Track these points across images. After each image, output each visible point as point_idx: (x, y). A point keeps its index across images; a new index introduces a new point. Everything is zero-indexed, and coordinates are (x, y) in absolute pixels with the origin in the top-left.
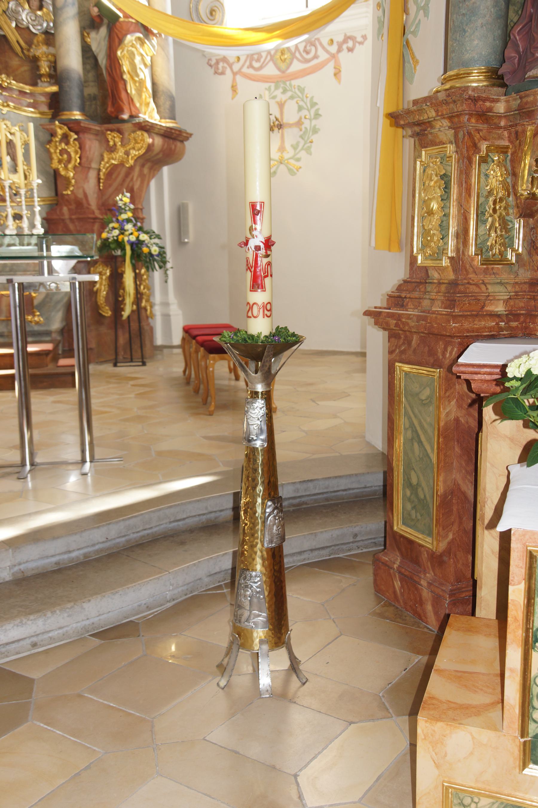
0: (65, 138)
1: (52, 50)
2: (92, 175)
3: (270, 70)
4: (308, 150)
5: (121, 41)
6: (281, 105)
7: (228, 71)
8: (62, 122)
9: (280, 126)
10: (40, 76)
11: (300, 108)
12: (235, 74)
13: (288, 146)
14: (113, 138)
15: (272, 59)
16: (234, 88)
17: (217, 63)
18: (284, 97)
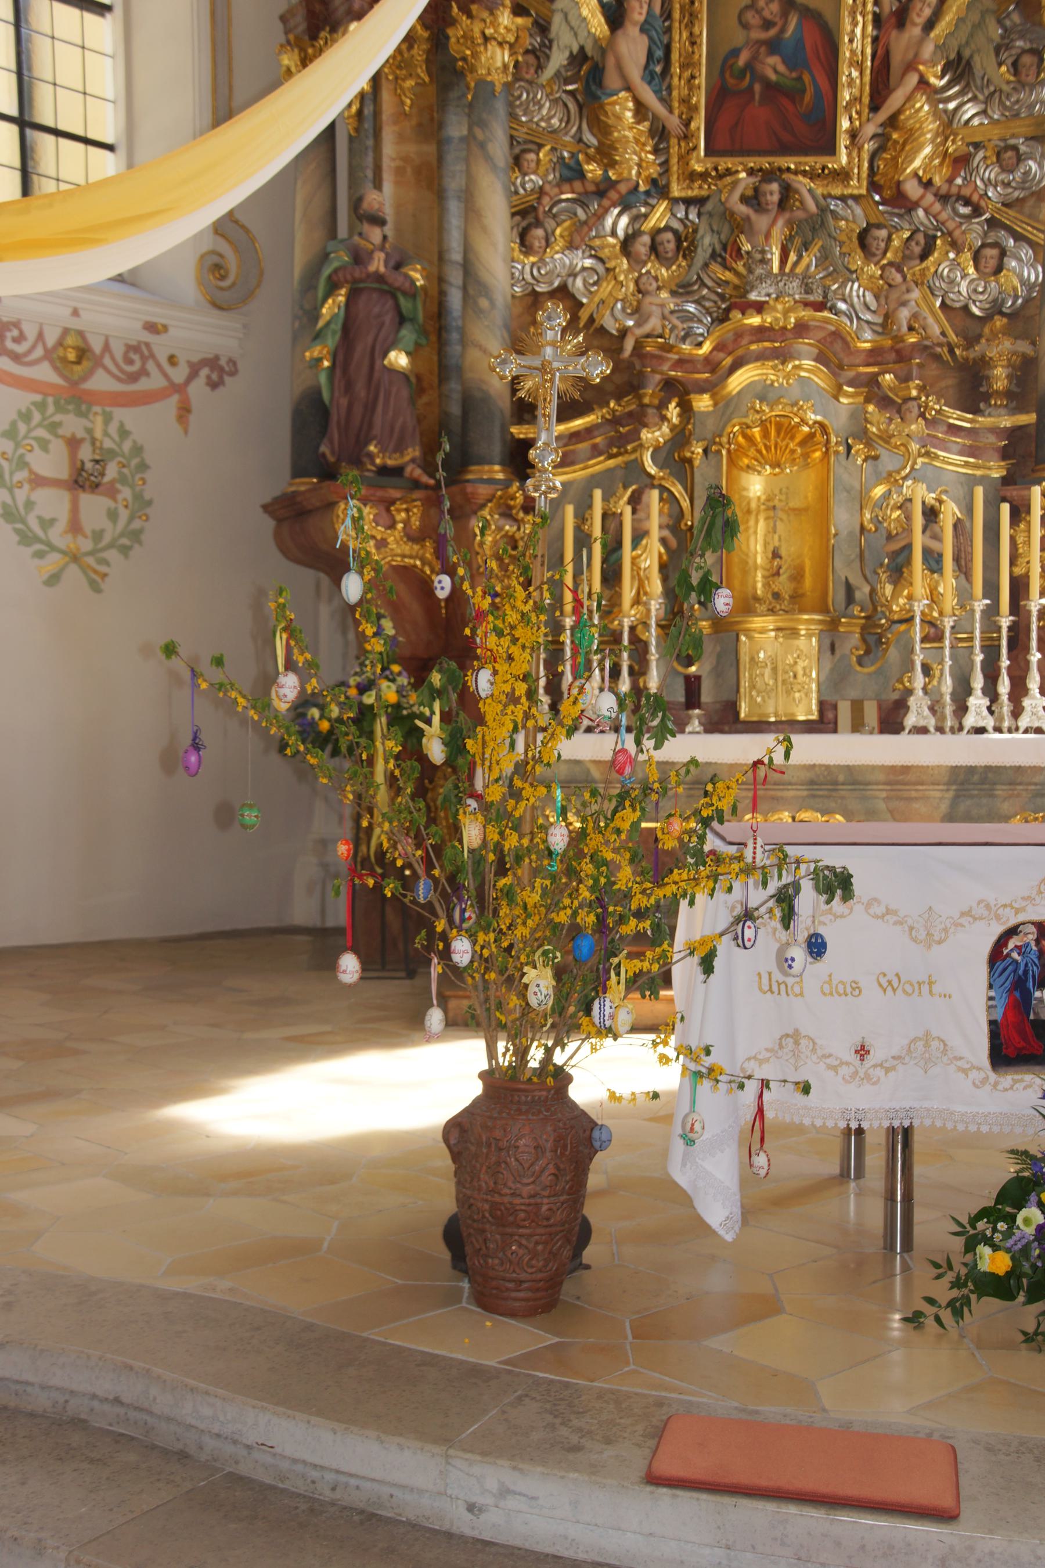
1: (1024, 347)
10: (986, 397)
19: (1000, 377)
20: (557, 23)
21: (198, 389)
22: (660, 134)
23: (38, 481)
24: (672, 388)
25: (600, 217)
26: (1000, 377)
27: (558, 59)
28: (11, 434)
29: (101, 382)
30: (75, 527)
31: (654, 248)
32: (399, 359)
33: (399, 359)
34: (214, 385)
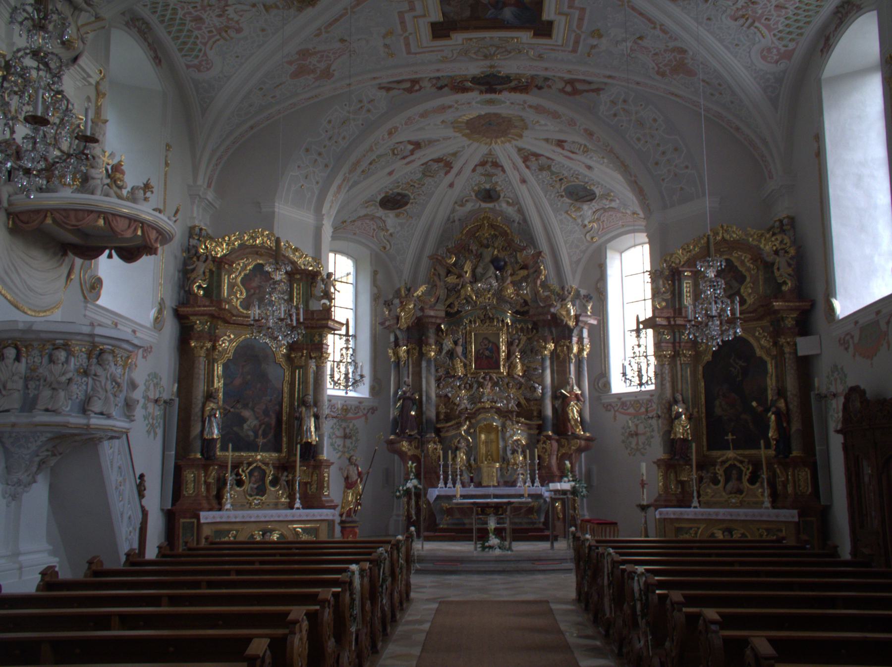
0: (544, 442)
2: (555, 457)
3: (631, 410)
4: (650, 445)
5: (568, 404)
6: (637, 426)
7: (612, 410)
8: (544, 436)
9: (637, 434)
11: (645, 428)
12: (615, 411)
13: (640, 443)
14: (563, 441)
15: (632, 406)
16: (615, 418)
17: (607, 406)
18: (638, 422)
19: (535, 414)
20: (444, 345)
21: (369, 414)
22: (465, 366)
23: (337, 437)
24: (466, 419)
25: (453, 382)
26: (535, 414)
27: (444, 352)
28: (332, 428)
29: (350, 415)
30: (344, 446)
31: (465, 387)
32: (413, 413)
33: (413, 413)
34: (373, 413)
